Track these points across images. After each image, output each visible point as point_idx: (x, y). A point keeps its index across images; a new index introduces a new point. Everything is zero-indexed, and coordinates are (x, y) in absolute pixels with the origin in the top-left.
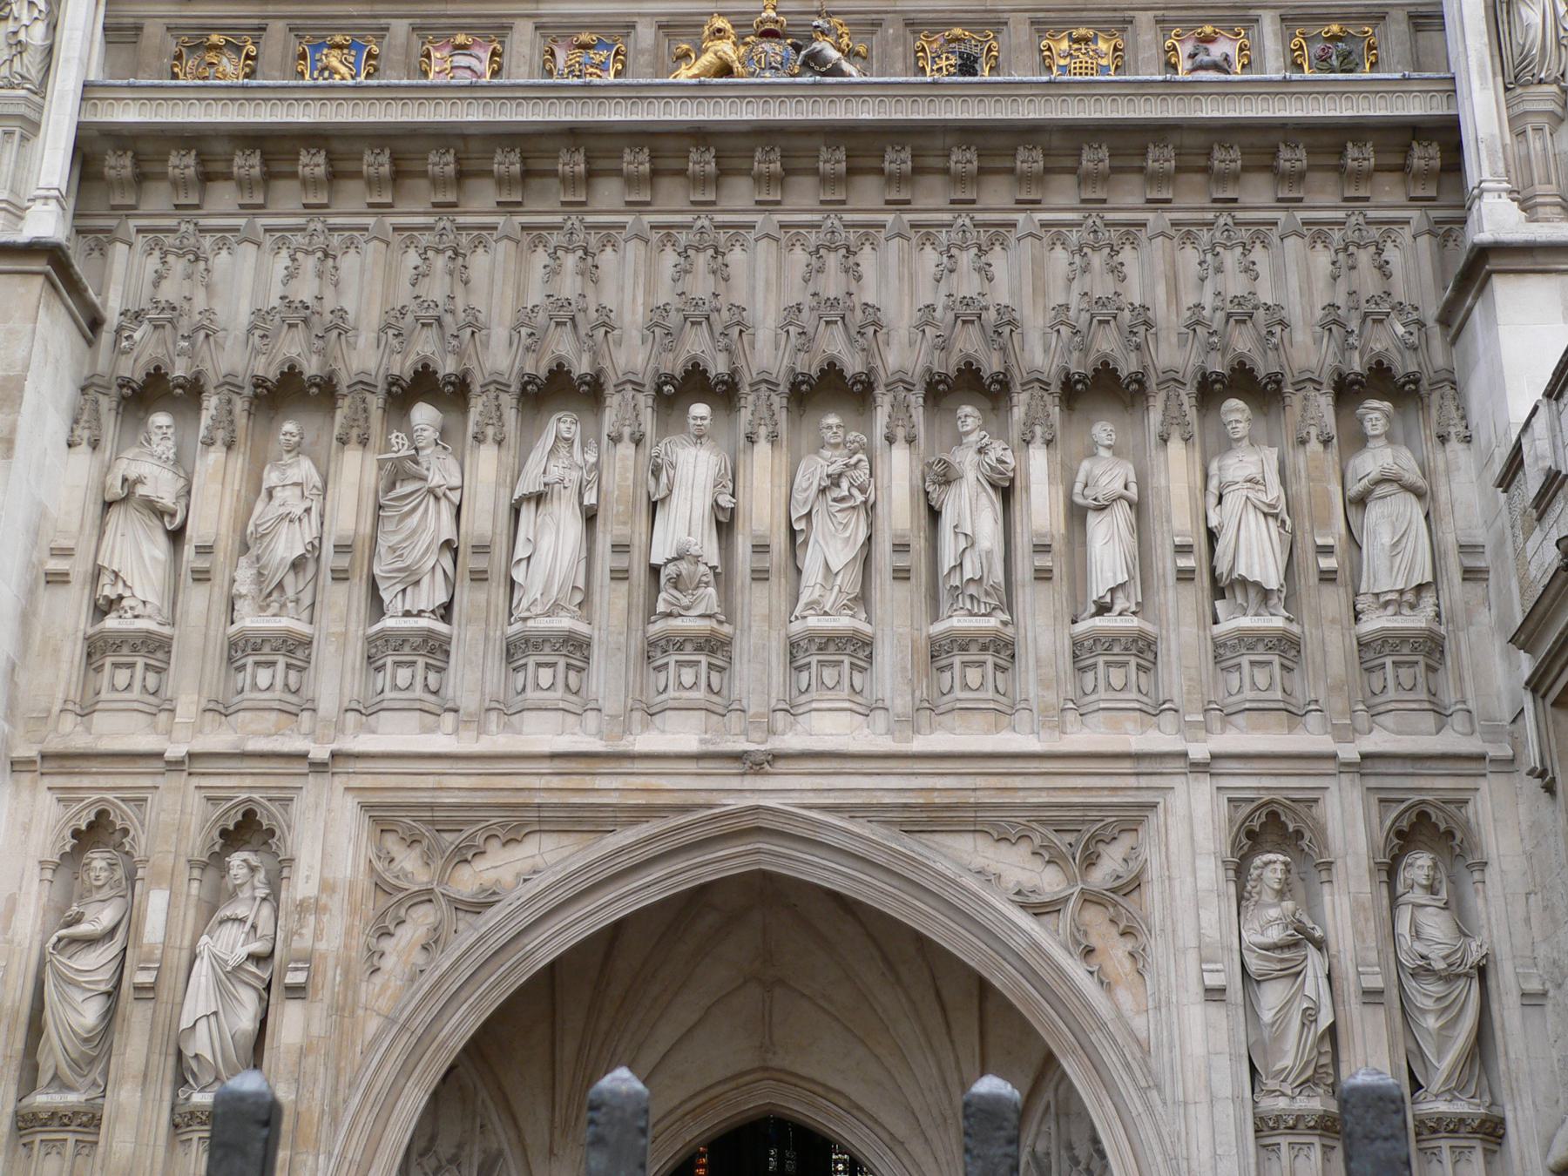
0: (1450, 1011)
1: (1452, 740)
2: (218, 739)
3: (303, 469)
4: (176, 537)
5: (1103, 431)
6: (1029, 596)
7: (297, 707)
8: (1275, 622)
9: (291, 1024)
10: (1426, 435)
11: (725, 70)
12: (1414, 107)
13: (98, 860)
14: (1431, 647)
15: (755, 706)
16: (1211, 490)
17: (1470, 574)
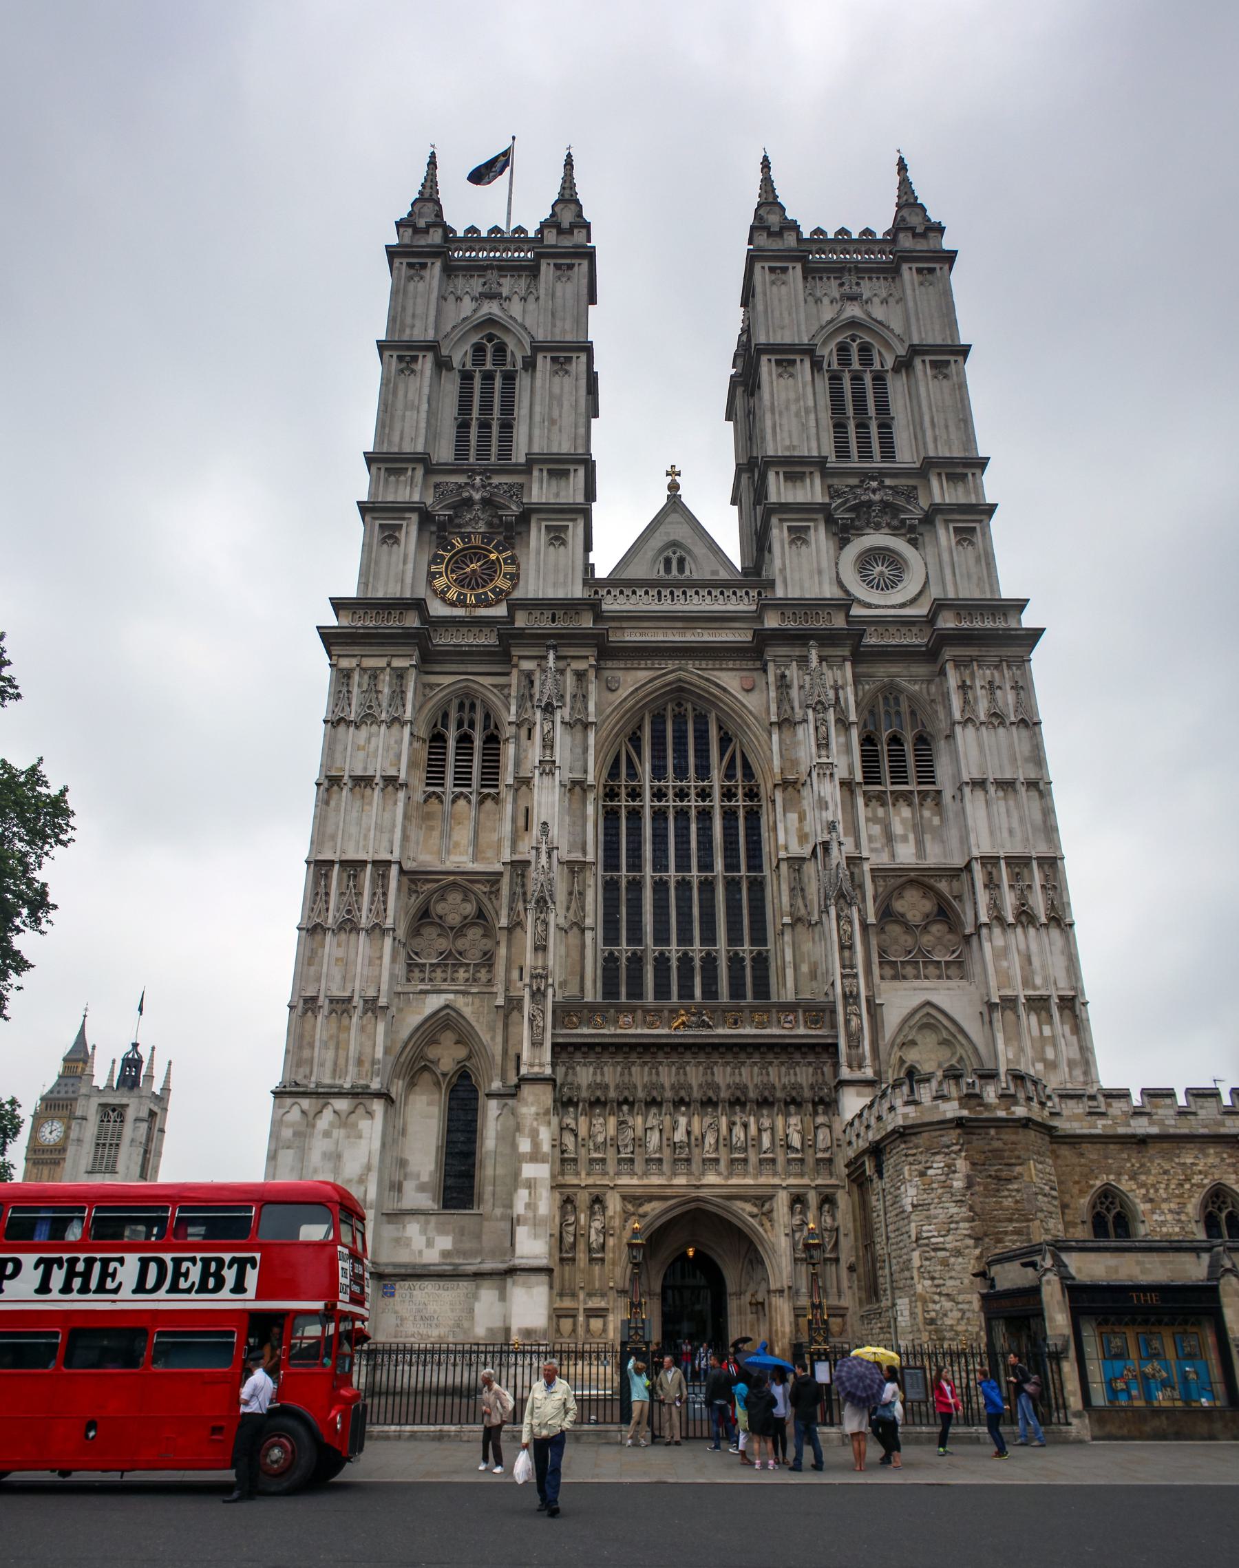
0: (830, 1237)
1: (833, 1181)
2: (590, 1181)
3: (601, 1120)
4: (576, 1136)
5: (765, 1112)
6: (750, 1149)
7: (605, 1173)
8: (799, 1156)
9: (611, 1242)
10: (830, 1113)
11: (683, 1023)
12: (830, 1041)
13: (569, 1207)
14: (830, 1161)
15: (696, 1173)
16: (787, 1125)
17: (839, 1146)
